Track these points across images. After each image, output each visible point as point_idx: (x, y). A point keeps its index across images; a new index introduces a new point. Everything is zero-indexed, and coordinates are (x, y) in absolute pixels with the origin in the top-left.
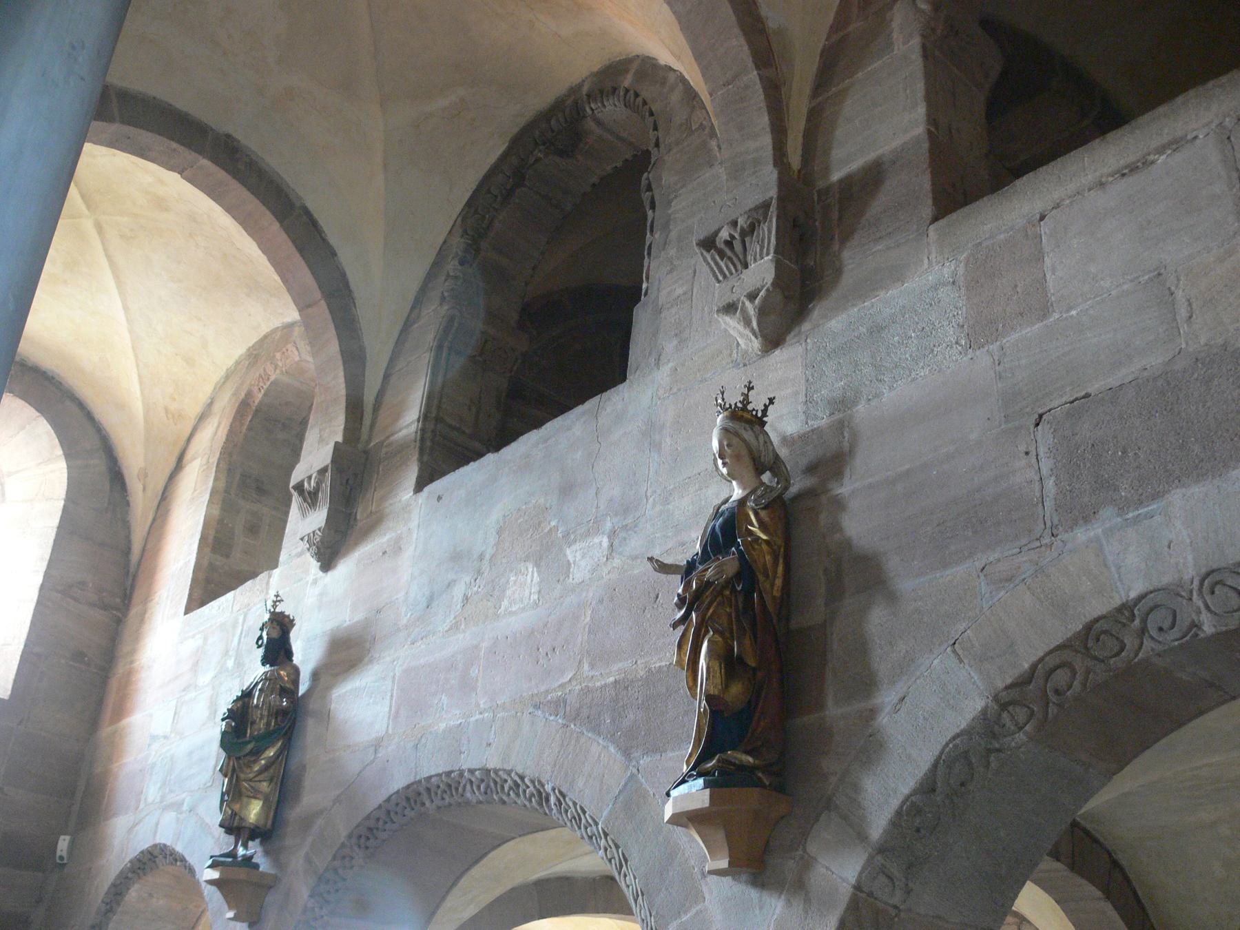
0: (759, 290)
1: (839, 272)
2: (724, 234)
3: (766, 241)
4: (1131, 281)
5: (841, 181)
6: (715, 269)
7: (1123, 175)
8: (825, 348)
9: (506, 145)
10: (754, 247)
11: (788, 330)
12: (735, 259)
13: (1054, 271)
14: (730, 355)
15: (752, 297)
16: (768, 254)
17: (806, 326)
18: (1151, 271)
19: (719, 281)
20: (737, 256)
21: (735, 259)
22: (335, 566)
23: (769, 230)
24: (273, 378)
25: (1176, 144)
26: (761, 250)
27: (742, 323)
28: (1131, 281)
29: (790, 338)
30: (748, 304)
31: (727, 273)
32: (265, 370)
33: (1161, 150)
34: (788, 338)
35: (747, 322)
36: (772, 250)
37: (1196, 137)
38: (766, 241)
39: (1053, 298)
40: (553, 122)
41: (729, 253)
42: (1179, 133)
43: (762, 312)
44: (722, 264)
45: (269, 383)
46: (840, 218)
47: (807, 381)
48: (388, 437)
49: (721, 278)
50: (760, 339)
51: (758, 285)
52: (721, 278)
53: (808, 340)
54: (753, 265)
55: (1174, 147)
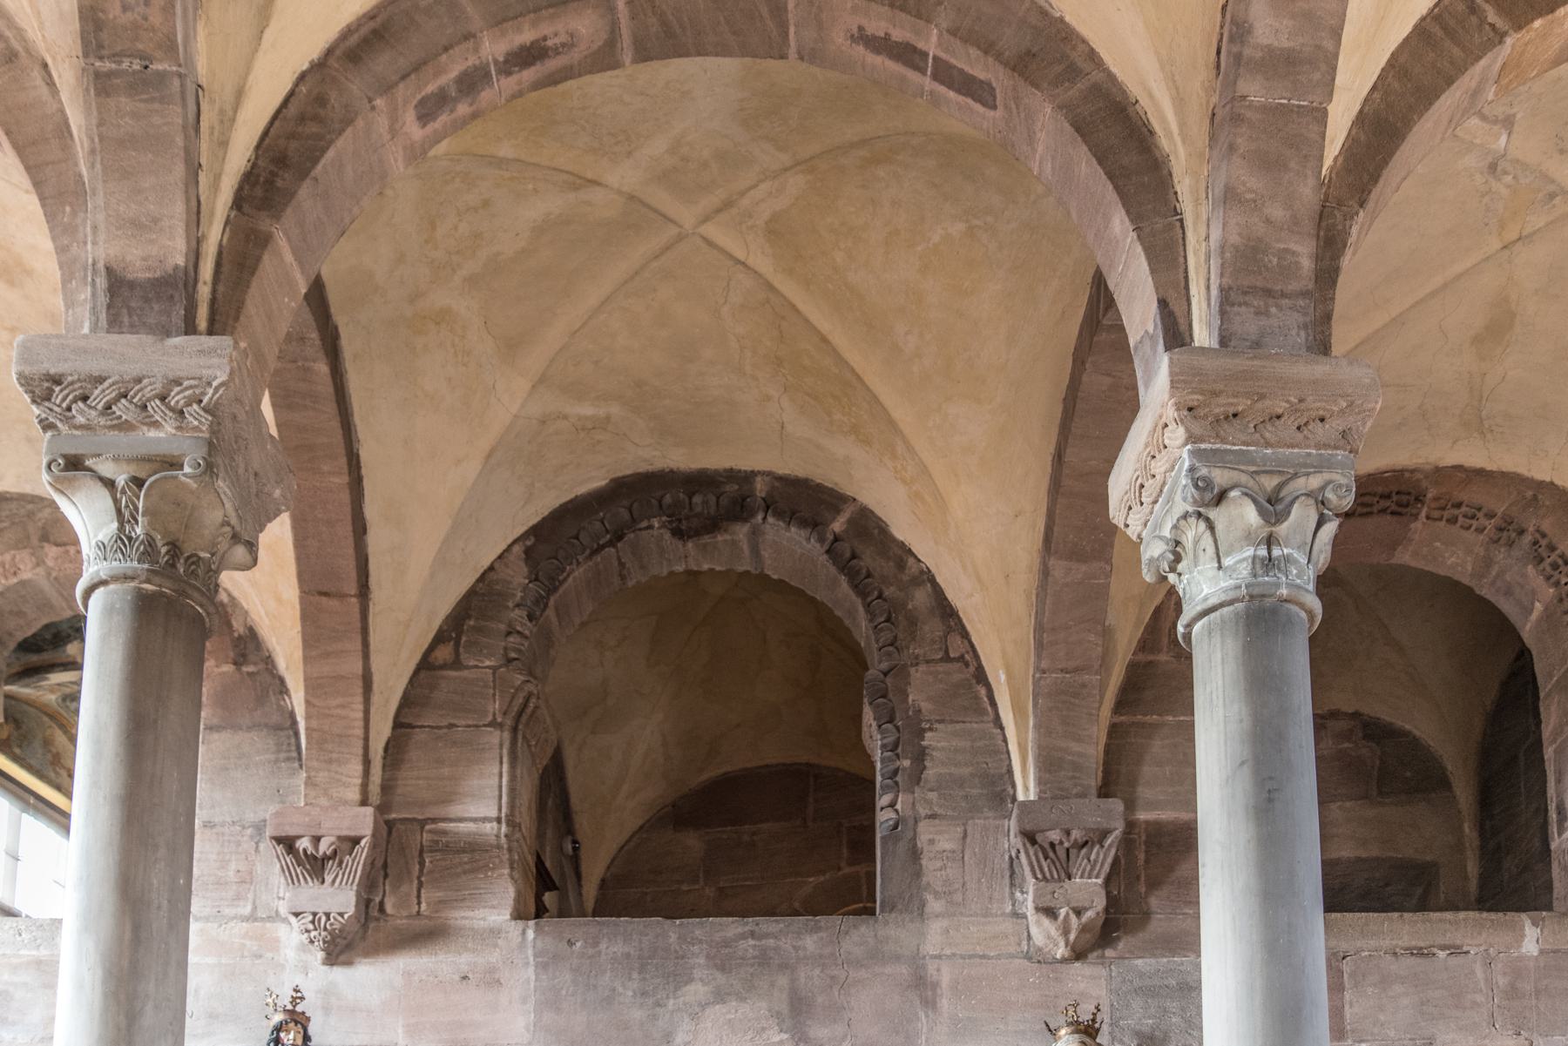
0: (1086, 909)
1: (1146, 915)
2: (1054, 836)
3: (1099, 865)
4: (1410, 1039)
5: (1147, 822)
6: (1035, 863)
7: (1412, 954)
8: (1131, 982)
9: (603, 483)
10: (1080, 863)
11: (1092, 949)
12: (1058, 864)
13: (1351, 1005)
14: (1019, 945)
15: (1078, 912)
16: (1097, 877)
17: (1109, 953)
18: (1424, 1039)
19: (1037, 878)
20: (1060, 862)
21: (1058, 864)
22: (349, 963)
23: (1104, 856)
24: (26, 575)
25: (1456, 950)
26: (1092, 870)
27: (1060, 931)
28: (1410, 1039)
29: (1093, 956)
30: (1073, 917)
31: (1048, 875)
32: (14, 558)
33: (1443, 948)
34: (1090, 956)
35: (1066, 932)
36: (1103, 876)
37: (1467, 952)
38: (1099, 865)
39: (1348, 1027)
40: (697, 499)
41: (1051, 854)
42: (1458, 942)
43: (1084, 929)
44: (1045, 864)
45: (15, 580)
46: (1147, 861)
47: (1112, 1005)
48: (434, 820)
49: (1039, 876)
50: (1069, 948)
51: (1087, 904)
52: (1039, 876)
53: (1112, 967)
54: (1078, 880)
55: (1453, 951)
